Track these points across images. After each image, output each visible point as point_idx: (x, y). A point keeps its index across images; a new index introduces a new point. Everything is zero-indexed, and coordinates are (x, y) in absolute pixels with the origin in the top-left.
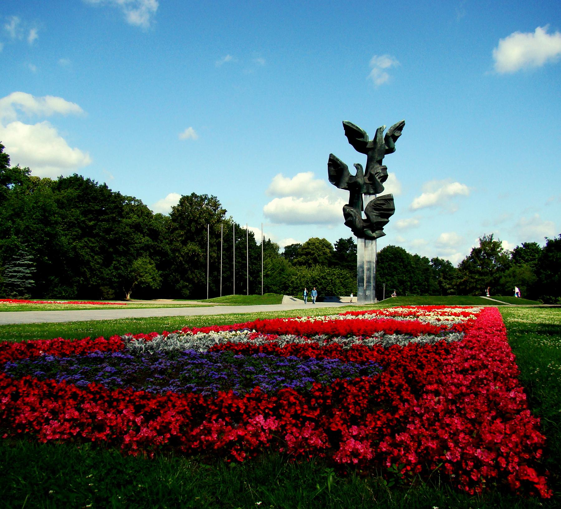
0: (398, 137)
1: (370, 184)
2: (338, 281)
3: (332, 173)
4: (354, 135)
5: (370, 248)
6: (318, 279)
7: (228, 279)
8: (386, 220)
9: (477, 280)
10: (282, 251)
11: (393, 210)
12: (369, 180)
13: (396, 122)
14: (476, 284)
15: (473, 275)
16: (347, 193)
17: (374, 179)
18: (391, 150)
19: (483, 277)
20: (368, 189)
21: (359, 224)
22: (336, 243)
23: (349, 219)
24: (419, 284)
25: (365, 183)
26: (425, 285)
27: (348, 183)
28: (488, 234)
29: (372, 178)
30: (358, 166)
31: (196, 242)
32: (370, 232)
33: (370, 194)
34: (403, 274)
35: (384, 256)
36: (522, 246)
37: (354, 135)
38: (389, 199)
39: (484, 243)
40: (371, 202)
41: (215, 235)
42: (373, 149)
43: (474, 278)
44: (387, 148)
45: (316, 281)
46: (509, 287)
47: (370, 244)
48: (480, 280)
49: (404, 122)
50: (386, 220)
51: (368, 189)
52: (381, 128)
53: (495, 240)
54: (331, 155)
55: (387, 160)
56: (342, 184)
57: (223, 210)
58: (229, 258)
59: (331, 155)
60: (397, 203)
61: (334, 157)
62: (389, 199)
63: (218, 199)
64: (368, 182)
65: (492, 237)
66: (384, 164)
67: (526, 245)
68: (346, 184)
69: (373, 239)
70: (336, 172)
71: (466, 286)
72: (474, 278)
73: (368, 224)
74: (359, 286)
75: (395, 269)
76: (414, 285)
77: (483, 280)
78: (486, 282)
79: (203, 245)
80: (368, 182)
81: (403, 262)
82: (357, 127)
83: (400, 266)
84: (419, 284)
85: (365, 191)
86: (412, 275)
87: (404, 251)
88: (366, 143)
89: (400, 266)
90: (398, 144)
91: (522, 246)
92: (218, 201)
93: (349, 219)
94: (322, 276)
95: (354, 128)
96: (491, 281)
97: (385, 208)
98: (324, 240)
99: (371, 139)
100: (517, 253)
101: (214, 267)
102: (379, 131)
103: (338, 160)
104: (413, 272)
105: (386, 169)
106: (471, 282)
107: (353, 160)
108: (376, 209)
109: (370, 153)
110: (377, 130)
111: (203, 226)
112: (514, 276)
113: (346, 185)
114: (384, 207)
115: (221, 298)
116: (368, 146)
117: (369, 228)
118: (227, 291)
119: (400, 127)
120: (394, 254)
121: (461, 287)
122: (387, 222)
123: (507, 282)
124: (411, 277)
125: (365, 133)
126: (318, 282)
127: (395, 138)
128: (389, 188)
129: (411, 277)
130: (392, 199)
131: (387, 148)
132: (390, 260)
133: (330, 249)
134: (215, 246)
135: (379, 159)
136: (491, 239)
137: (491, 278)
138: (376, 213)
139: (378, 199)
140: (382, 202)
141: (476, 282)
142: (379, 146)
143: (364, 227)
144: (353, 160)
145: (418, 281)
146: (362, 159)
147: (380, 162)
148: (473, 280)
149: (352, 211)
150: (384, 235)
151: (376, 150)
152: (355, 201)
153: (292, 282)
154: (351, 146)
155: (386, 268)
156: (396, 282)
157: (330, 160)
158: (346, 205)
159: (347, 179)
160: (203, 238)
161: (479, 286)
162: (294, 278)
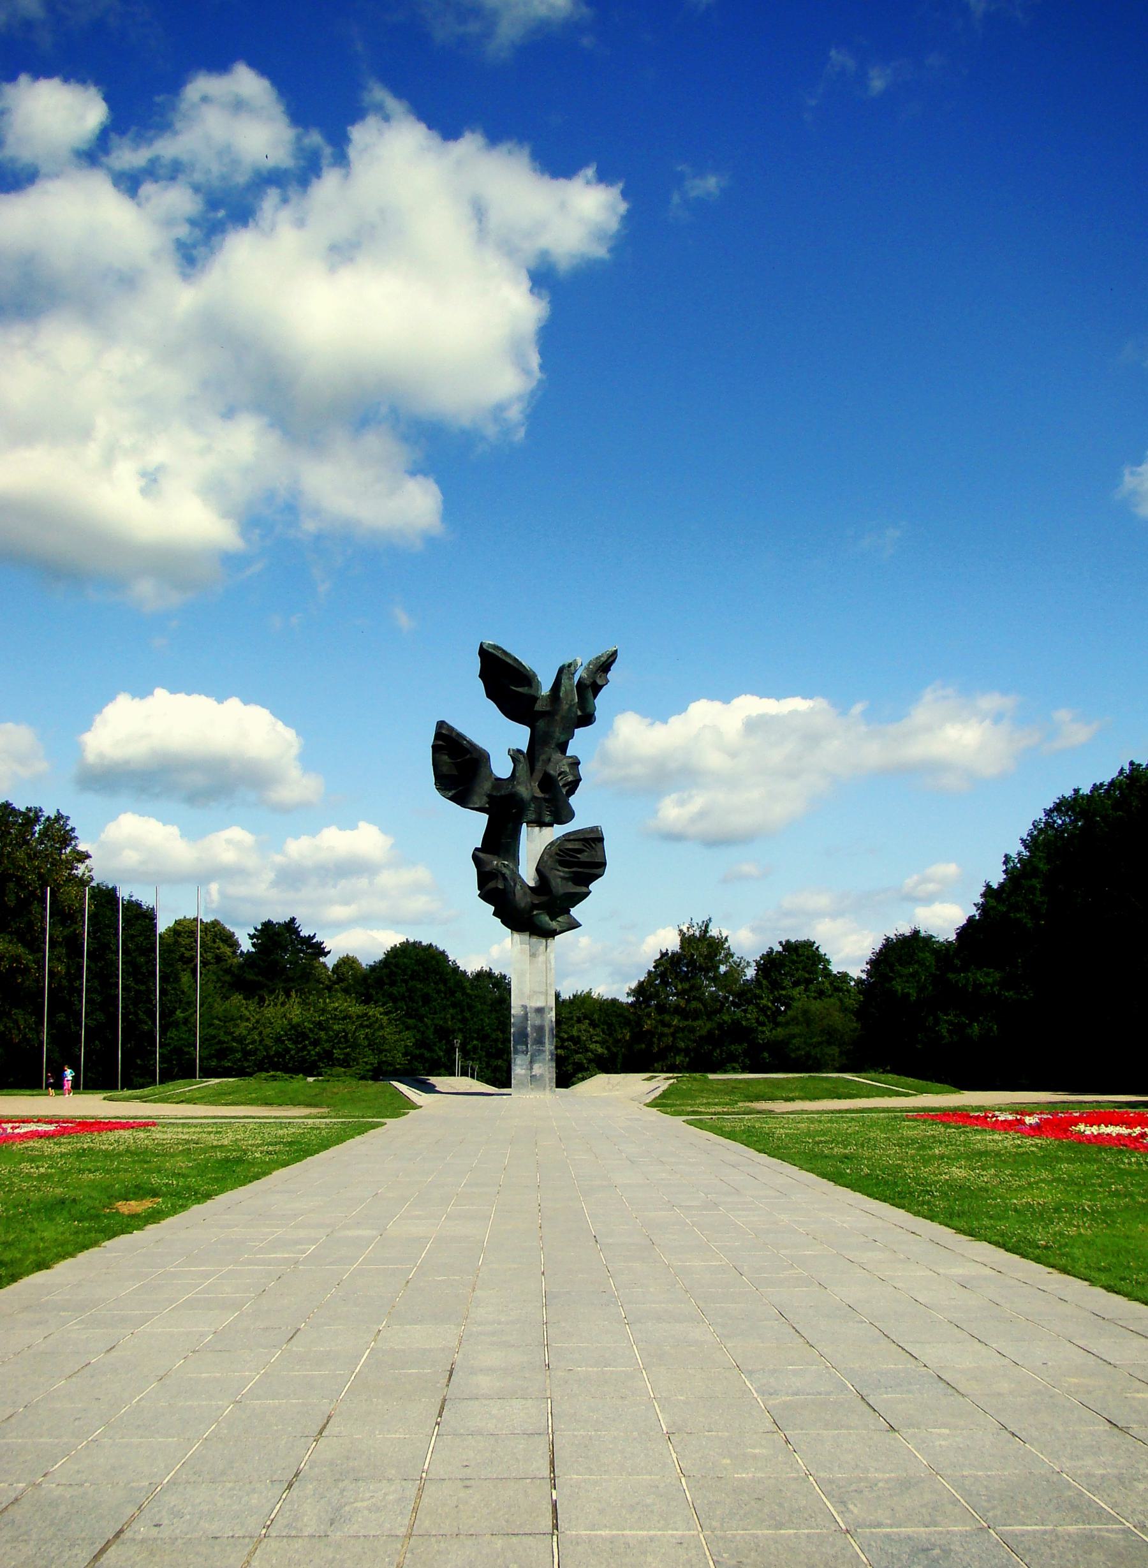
0: (602, 686)
1: (545, 799)
2: (361, 1034)
3: (445, 770)
4: (503, 678)
5: (541, 958)
6: (311, 1030)
7: (102, 1033)
8: (584, 889)
9: (679, 1029)
10: (330, 961)
11: (603, 864)
12: (542, 791)
13: (600, 650)
14: (675, 1038)
15: (667, 1018)
18: (587, 719)
19: (689, 1022)
20: (539, 814)
21: (522, 900)
22: (252, 932)
23: (491, 885)
24: (484, 1038)
25: (534, 798)
26: (496, 1041)
27: (489, 796)
28: (699, 919)
29: (547, 783)
30: (515, 755)
31: (11, 933)
32: (547, 918)
33: (542, 824)
35: (397, 966)
36: (780, 949)
37: (503, 678)
38: (593, 840)
39: (687, 941)
40: (552, 844)
41: (66, 916)
42: (548, 715)
43: (669, 1026)
44: (579, 713)
45: (304, 1036)
46: (798, 1049)
47: (542, 948)
48: (682, 1030)
49: (615, 653)
50: (584, 889)
51: (539, 814)
52: (570, 665)
53: (713, 932)
54: (441, 725)
55: (580, 743)
56: (475, 798)
57: (79, 853)
58: (103, 977)
59: (441, 725)
60: (610, 848)
61: (451, 729)
62: (593, 840)
63: (71, 824)
64: (539, 794)
65: (707, 926)
67: (788, 946)
68: (485, 799)
69: (550, 934)
70: (456, 766)
71: (651, 1044)
72: (669, 1026)
73: (544, 899)
74: (516, 1052)
75: (426, 999)
76: (472, 1039)
77: (692, 1030)
78: (698, 1034)
79: (35, 946)
80: (539, 794)
81: (445, 982)
83: (438, 992)
84: (484, 1038)
85: (533, 817)
86: (468, 1015)
88: (534, 699)
89: (438, 992)
90: (601, 703)
91: (780, 949)
92: (73, 830)
93: (491, 885)
94: (320, 1023)
95: (510, 662)
96: (710, 1032)
97: (581, 861)
98: (215, 923)
99: (545, 689)
100: (770, 964)
101: (63, 1000)
102: (564, 671)
103: (461, 736)
104: (470, 1007)
105: (579, 763)
106: (662, 1035)
107: (501, 740)
108: (563, 863)
109: (541, 724)
110: (561, 670)
111: (33, 893)
112: (808, 1023)
113: (482, 801)
114: (583, 857)
115: (158, 1089)
116: (538, 707)
117: (537, 909)
118: (186, 1072)
119: (605, 665)
120: (419, 962)
121: (637, 1047)
122: (586, 894)
123: (794, 1036)
124: (464, 1020)
125: (535, 675)
126: (308, 1038)
127: (597, 689)
128: (586, 810)
129: (464, 1020)
130: (601, 840)
131: (579, 713)
132: (412, 978)
133: (231, 946)
134: (60, 944)
135: (563, 738)
136: (706, 931)
137: (709, 1025)
138: (562, 872)
139: (567, 838)
140: (577, 845)
141: (673, 1034)
142: (565, 707)
143: (535, 906)
144: (501, 740)
145: (483, 1029)
146: (520, 736)
147: (563, 747)
148: (666, 1030)
150: (574, 925)
151: (558, 718)
152: (498, 843)
153: (240, 1040)
155: (403, 998)
156: (430, 1033)
157: (438, 736)
158: (476, 849)
159: (487, 786)
160: (30, 925)
161: (682, 1045)
162: (242, 1029)
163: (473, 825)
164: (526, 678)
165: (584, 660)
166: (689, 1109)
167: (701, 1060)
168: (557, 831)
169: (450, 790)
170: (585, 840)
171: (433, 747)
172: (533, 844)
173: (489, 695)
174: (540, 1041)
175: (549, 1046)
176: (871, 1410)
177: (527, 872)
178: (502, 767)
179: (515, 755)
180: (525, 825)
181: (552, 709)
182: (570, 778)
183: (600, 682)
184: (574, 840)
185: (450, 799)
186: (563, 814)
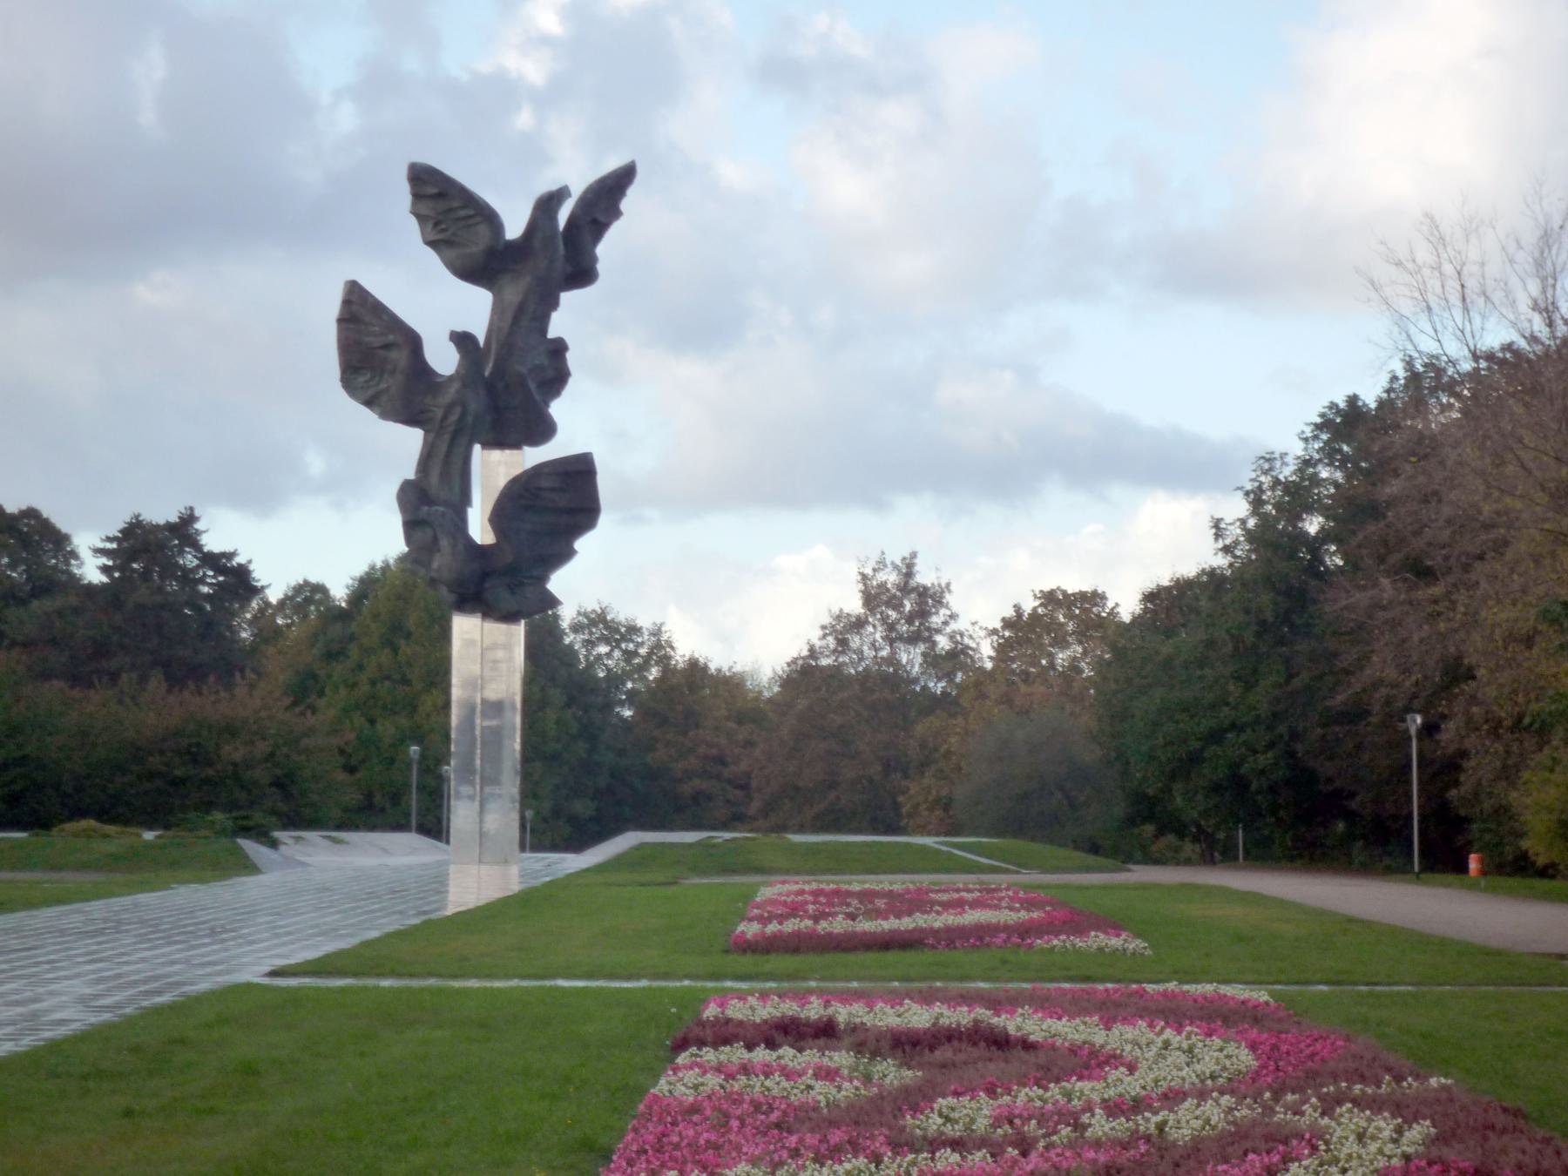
17: (512, 385)
28: (895, 556)
30: (462, 340)
34: (636, 755)
55: (571, 318)
70: (374, 353)
90: (607, 250)
97: (561, 504)
102: (548, 204)
107: (445, 310)
128: (575, 422)
144: (445, 310)
146: (473, 308)
157: (347, 302)
165: (577, 175)
166: (955, 986)
168: (533, 456)
170: (567, 474)
172: (493, 470)
180: (477, 448)
182: (550, 373)
183: (602, 219)
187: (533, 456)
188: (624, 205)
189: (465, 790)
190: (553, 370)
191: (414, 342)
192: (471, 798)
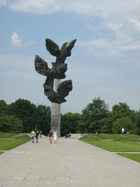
4: (51, 46)
16: (46, 77)
17: (60, 71)
30: (53, 64)
37: (51, 46)
38: (70, 83)
53: (101, 99)
54: (37, 56)
55: (68, 61)
59: (37, 56)
62: (70, 83)
66: (65, 63)
70: (40, 65)
74: (52, 128)
82: (54, 42)
87: (29, 102)
90: (73, 51)
95: (53, 43)
97: (67, 87)
100: (115, 108)
102: (65, 44)
103: (41, 59)
107: (50, 60)
128: (69, 75)
139: (64, 82)
146: (54, 59)
149: (49, 87)
150: (65, 101)
154: (48, 52)
157: (36, 58)
163: (43, 78)
164: (56, 46)
165: (69, 41)
167: (91, 131)
169: (39, 71)
171: (35, 61)
172: (56, 83)
173: (48, 50)
174: (56, 126)
175: (59, 127)
176: (74, 139)
177: (55, 89)
178: (50, 66)
179: (53, 64)
180: (55, 79)
181: (62, 53)
183: (72, 47)
184: (65, 83)
185: (39, 73)
186: (64, 77)
187: (62, 80)
188: (74, 45)
189: (53, 127)
190: (65, 69)
191: (47, 64)
192: (54, 129)
